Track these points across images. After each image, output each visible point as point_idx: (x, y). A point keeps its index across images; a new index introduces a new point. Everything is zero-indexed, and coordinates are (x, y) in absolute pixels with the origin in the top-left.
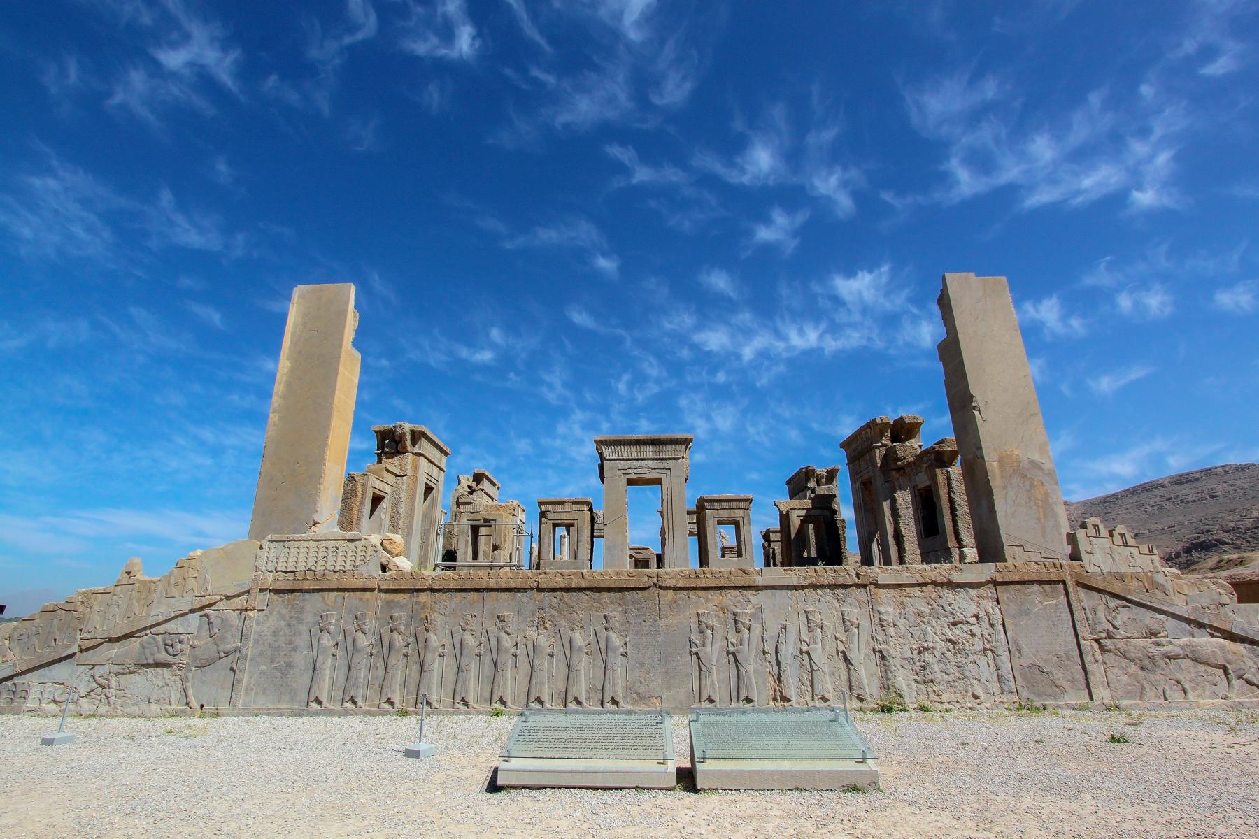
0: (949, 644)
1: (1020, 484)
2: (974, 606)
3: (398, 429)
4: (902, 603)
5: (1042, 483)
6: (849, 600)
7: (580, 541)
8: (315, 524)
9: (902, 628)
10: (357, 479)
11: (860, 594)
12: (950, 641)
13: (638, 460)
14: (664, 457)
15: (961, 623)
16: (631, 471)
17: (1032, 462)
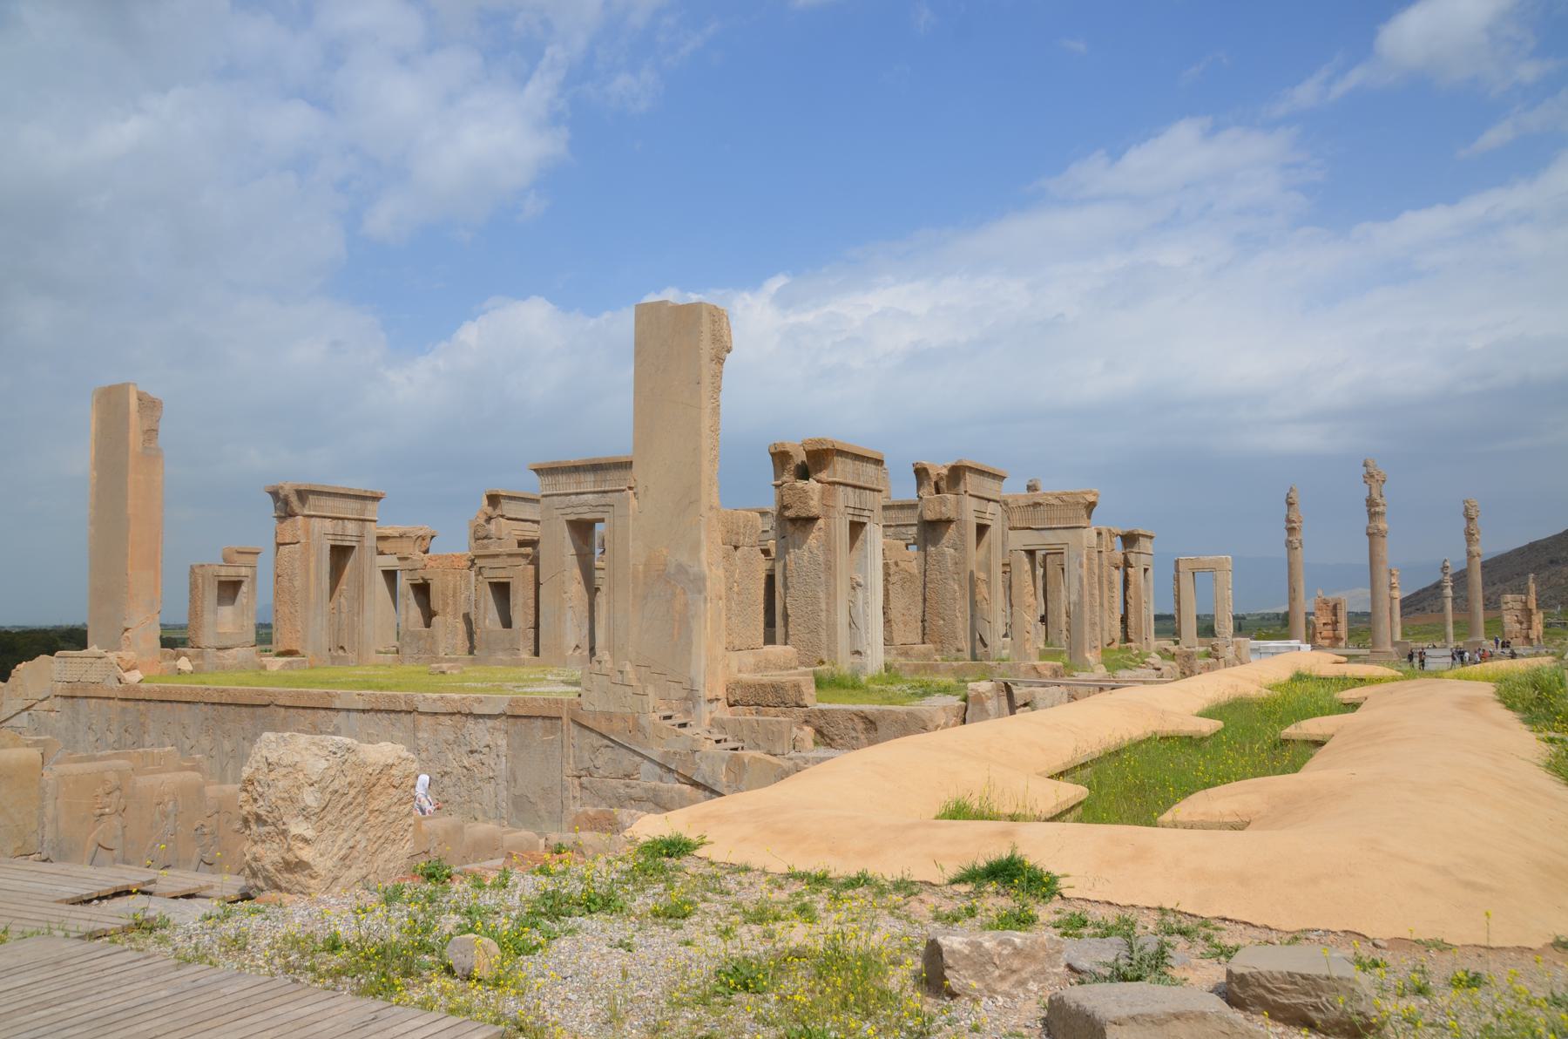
0: (465, 770)
1: (662, 594)
2: (488, 737)
3: (280, 491)
4: (436, 730)
5: (685, 591)
6: (398, 725)
7: (515, 605)
8: (126, 630)
9: (432, 753)
10: (197, 570)
11: (406, 719)
12: (465, 767)
13: (577, 494)
14: (607, 489)
15: (476, 751)
16: (569, 510)
17: (681, 569)
